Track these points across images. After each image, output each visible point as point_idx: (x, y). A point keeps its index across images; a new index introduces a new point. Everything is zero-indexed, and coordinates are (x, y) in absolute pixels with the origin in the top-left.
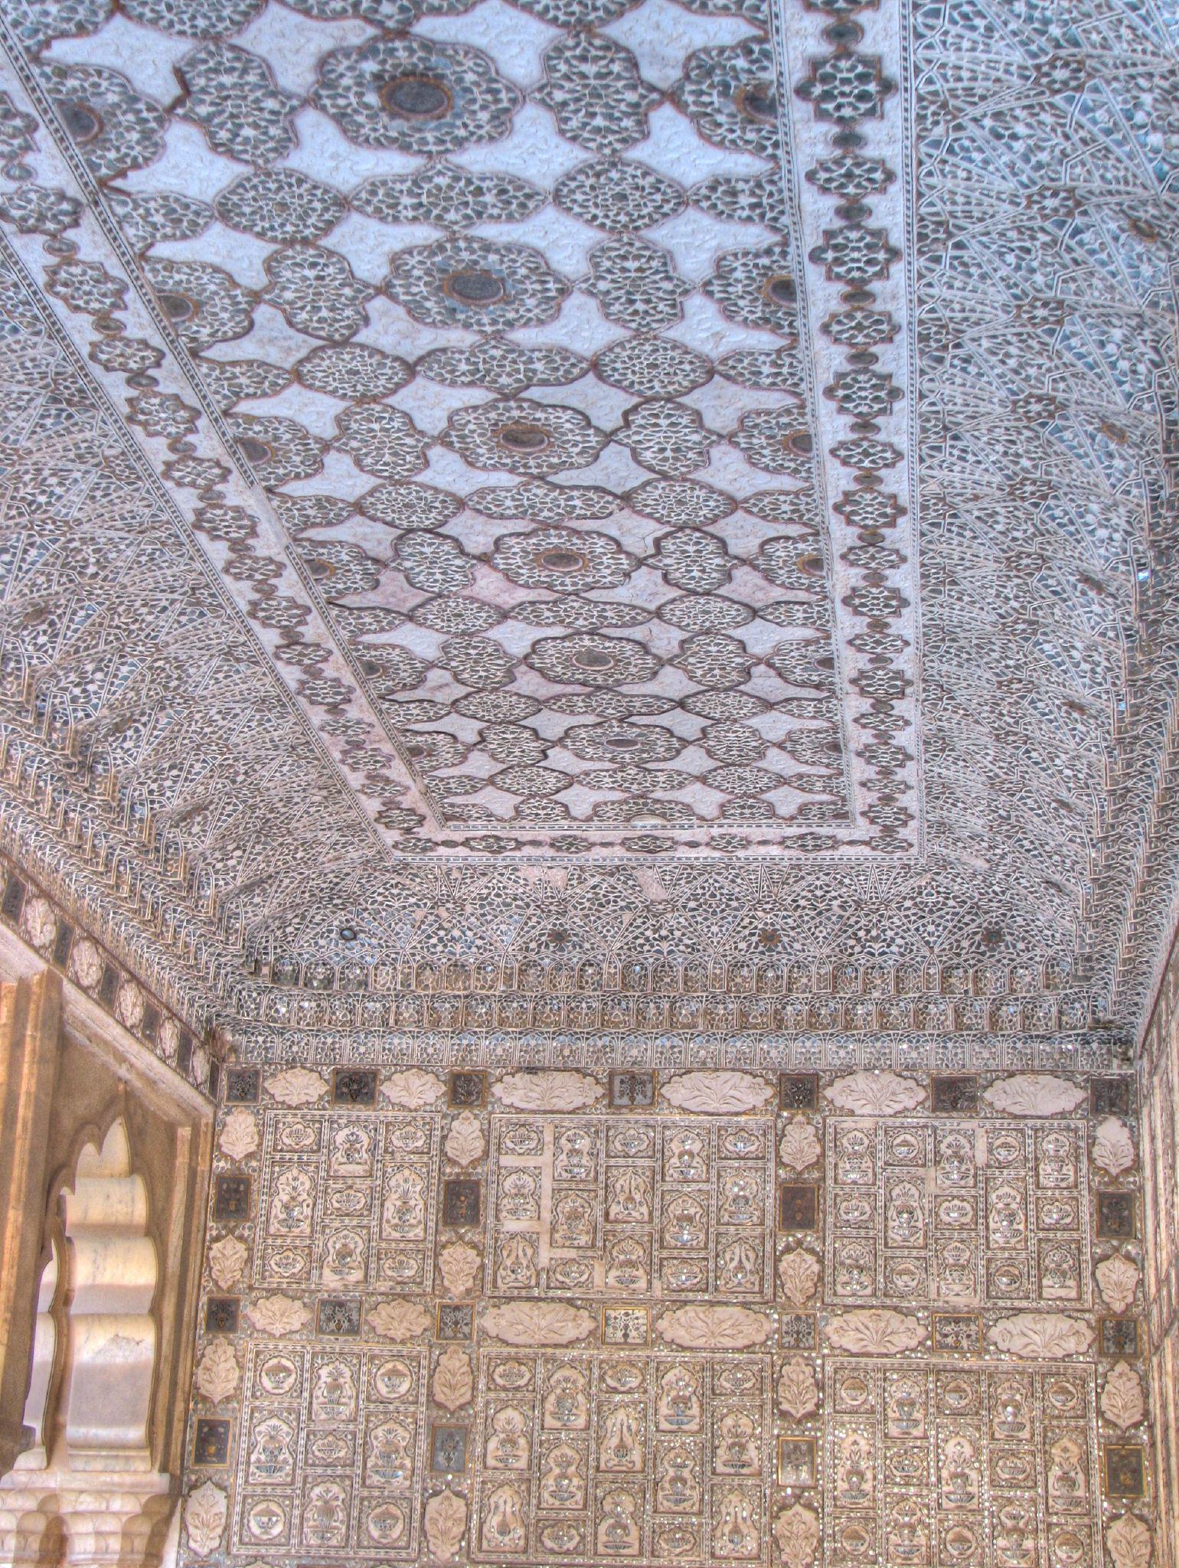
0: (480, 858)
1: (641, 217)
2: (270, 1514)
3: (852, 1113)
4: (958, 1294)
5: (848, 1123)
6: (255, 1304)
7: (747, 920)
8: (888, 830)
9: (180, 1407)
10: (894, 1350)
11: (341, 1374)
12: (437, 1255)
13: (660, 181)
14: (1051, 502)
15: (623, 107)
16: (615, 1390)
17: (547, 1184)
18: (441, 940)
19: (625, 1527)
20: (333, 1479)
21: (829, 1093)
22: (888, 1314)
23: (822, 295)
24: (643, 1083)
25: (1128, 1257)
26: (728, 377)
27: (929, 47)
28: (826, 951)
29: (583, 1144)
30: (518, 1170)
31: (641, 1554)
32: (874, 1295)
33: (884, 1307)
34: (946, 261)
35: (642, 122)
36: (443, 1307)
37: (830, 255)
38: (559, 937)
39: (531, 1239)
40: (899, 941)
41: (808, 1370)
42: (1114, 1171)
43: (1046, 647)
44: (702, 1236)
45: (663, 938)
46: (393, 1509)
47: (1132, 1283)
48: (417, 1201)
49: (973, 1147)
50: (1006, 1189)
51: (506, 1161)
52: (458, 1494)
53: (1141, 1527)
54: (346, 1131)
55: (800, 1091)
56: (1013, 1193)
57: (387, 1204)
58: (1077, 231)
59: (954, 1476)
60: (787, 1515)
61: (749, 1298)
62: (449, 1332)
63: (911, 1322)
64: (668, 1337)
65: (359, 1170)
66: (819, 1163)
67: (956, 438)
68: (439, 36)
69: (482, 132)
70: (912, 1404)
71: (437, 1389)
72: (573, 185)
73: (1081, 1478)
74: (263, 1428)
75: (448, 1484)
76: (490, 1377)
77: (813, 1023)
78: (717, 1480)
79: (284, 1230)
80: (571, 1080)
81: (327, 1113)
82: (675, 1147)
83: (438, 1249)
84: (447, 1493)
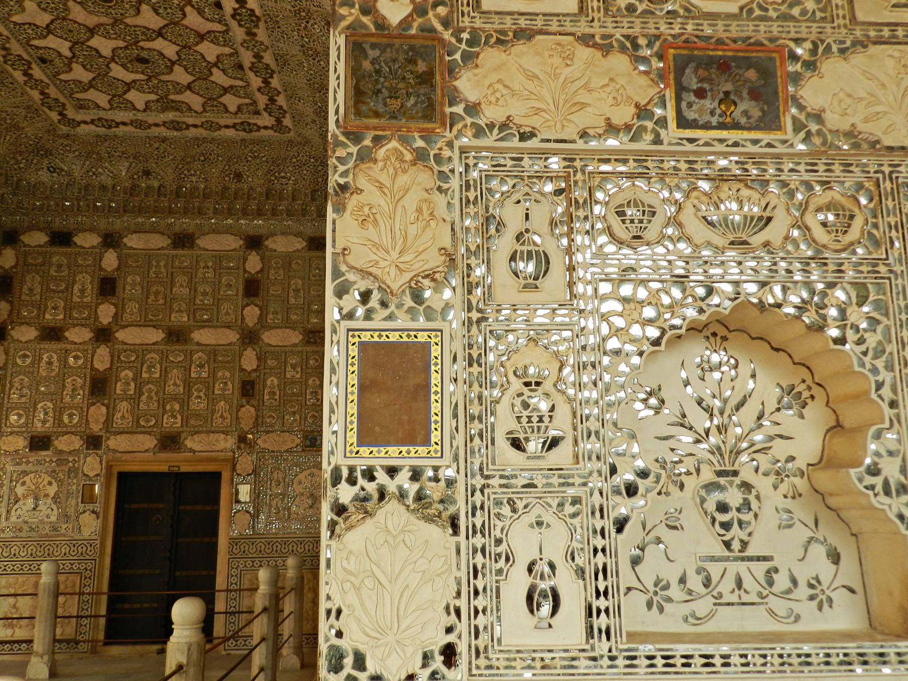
0: (102, 131)
7: (227, 167)
8: (279, 121)
11: (52, 357)
12: (96, 308)
18: (94, 173)
21: (266, 243)
22: (287, 330)
28: (262, 181)
31: (182, 426)
33: (286, 327)
38: (147, 173)
40: (293, 178)
45: (191, 175)
46: (74, 411)
52: (103, 404)
54: (57, 258)
55: (254, 243)
57: (75, 287)
66: (262, 270)
71: (95, 363)
76: (119, 358)
77: (259, 213)
80: (157, 236)
82: (202, 264)
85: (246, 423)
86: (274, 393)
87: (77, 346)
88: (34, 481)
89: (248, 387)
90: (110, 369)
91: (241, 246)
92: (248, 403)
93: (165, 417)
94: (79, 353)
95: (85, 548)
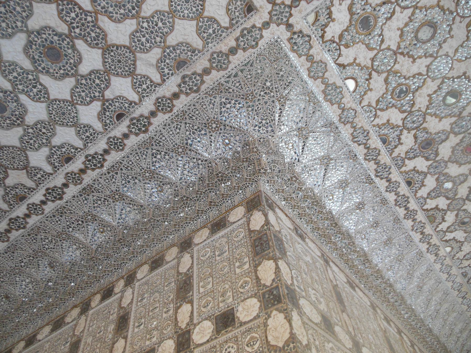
1: (62, 121)
13: (77, 117)
14: (64, 242)
15: (92, 95)
23: (76, 165)
26: (27, 172)
27: (164, 129)
34: (110, 175)
35: (91, 102)
37: (90, 158)
43: (17, 278)
58: (146, 183)
67: (61, 216)
68: (78, 47)
69: (56, 75)
72: (58, 102)
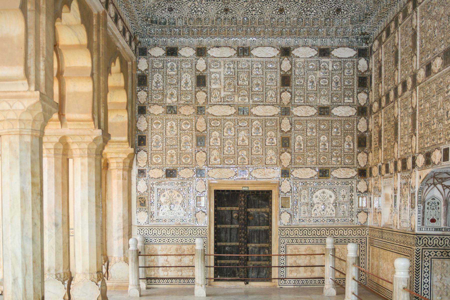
2: (158, 157)
3: (299, 57)
4: (325, 102)
5: (298, 60)
6: (150, 107)
9: (134, 132)
10: (309, 115)
12: (195, 94)
16: (241, 126)
17: (222, 76)
19: (244, 158)
20: (173, 149)
21: (293, 52)
22: (307, 107)
24: (246, 50)
25: (365, 92)
29: (232, 66)
30: (215, 73)
31: (248, 164)
32: (304, 102)
33: (307, 105)
36: (198, 107)
39: (219, 90)
41: (288, 121)
42: (363, 71)
44: (262, 89)
47: (366, 99)
48: (189, 81)
49: (328, 66)
50: (336, 76)
51: (212, 70)
52: (204, 152)
53: (365, 154)
54: (170, 63)
55: (286, 52)
56: (338, 77)
57: (182, 82)
59: (322, 144)
60: (283, 154)
61: (274, 103)
62: (199, 113)
63: (313, 108)
64: (254, 113)
65: (174, 73)
66: (291, 69)
70: (313, 128)
71: (197, 127)
73: (352, 144)
74: (154, 137)
75: (201, 149)
76: (210, 124)
77: (290, 34)
78: (266, 147)
79: (156, 89)
81: (165, 59)
82: (255, 66)
83: (196, 92)
84: (201, 151)
85: (286, 163)
86: (301, 145)
87: (186, 117)
88: (170, 194)
89: (286, 141)
90: (206, 130)
91: (278, 55)
92: (286, 150)
93: (239, 159)
94: (188, 122)
95: (192, 231)
